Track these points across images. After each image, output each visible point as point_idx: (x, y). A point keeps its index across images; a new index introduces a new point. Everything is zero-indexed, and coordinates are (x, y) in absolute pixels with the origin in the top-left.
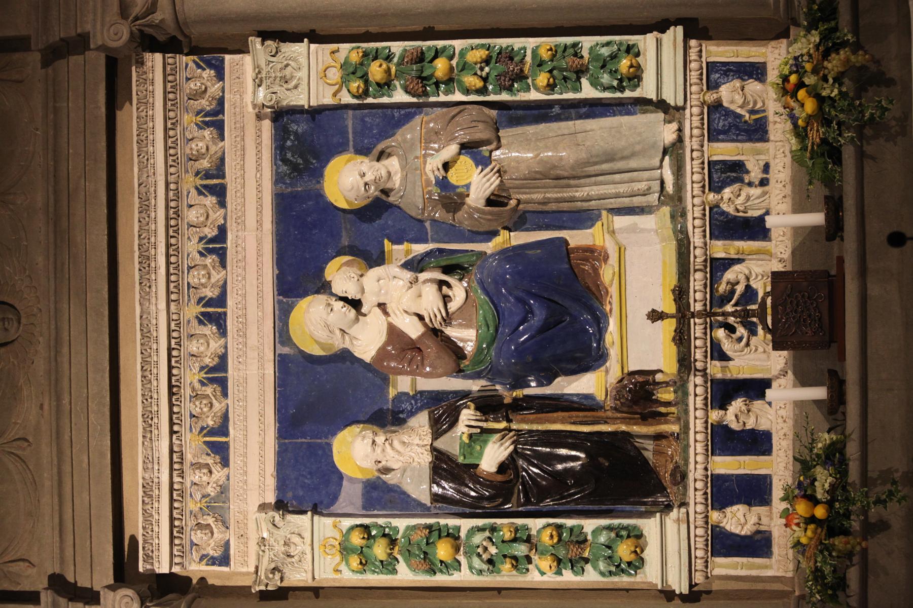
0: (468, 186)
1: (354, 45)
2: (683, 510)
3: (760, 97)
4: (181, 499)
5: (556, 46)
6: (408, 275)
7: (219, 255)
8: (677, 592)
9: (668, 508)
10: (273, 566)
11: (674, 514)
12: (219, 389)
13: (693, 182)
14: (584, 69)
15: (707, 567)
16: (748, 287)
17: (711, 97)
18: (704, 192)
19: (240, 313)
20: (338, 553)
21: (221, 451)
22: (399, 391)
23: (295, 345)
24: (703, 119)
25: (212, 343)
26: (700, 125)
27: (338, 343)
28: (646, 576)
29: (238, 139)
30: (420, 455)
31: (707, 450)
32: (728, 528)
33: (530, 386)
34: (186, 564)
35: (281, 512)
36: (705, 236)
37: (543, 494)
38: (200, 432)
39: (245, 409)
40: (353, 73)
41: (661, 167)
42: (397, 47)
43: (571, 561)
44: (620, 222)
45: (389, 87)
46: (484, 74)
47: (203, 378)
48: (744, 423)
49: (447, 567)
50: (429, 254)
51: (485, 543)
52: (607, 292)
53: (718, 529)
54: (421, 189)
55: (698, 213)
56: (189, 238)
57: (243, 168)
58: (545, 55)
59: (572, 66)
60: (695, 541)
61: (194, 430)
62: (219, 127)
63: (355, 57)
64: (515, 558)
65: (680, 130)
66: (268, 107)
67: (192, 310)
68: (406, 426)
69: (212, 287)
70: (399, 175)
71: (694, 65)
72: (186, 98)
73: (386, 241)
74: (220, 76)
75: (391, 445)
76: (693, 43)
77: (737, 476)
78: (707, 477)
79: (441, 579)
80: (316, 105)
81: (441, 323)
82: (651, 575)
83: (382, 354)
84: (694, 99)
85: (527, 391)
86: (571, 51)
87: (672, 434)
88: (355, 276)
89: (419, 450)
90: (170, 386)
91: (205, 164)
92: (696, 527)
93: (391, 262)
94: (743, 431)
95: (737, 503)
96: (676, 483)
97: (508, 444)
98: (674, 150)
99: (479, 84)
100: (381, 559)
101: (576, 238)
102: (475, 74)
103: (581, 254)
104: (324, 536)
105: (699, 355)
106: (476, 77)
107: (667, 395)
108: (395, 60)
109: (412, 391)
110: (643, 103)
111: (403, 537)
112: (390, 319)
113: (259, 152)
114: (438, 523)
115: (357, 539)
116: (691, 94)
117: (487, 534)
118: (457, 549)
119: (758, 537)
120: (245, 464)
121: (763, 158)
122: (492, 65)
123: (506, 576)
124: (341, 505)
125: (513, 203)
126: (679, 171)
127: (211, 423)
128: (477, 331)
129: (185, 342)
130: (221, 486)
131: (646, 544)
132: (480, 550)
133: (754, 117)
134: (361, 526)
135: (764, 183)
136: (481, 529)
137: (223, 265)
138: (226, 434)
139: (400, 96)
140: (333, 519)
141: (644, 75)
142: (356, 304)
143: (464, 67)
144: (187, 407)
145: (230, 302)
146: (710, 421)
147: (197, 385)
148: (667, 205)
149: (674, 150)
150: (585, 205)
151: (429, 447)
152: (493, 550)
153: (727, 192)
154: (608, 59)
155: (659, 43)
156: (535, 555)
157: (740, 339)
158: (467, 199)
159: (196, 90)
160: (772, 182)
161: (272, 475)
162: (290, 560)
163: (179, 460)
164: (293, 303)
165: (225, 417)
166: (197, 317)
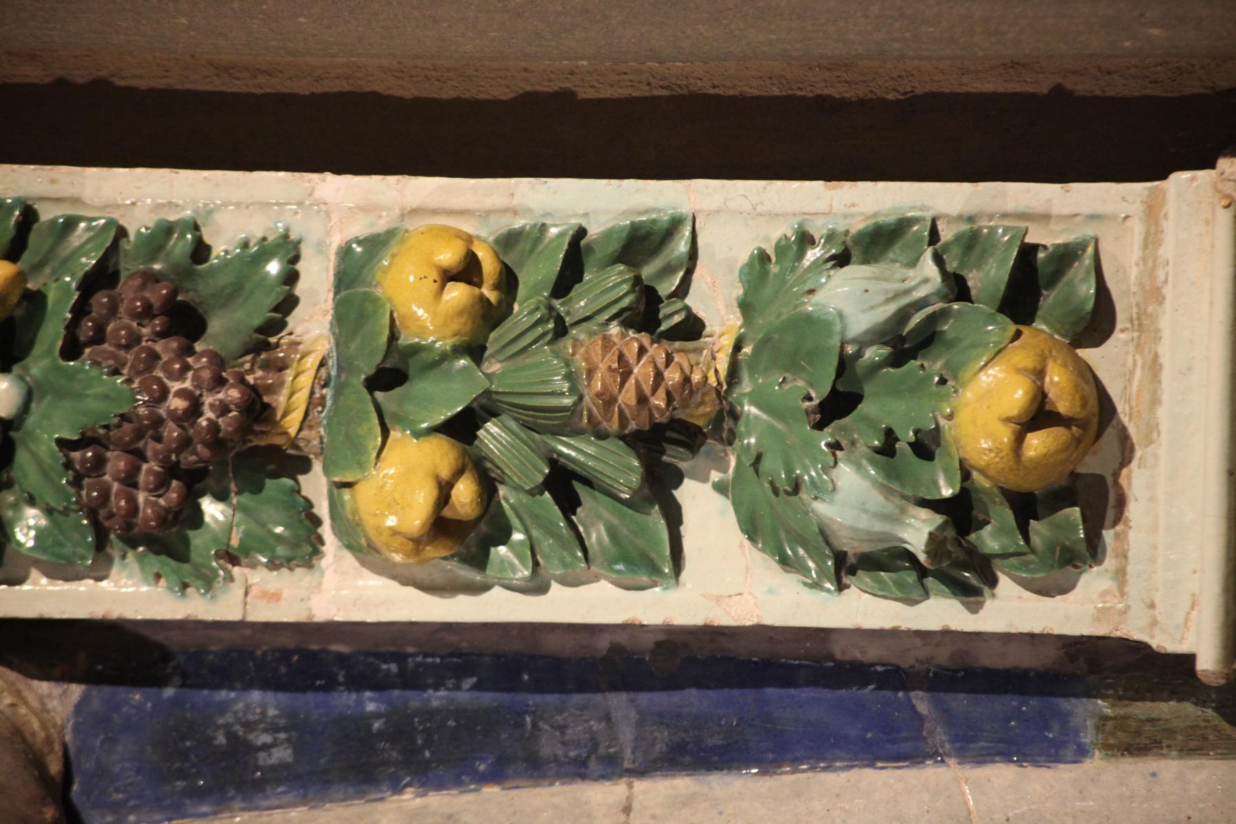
5: (508, 241)
14: (700, 414)
59: (608, 401)
154: (873, 354)
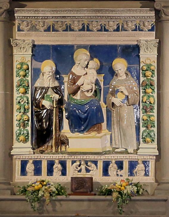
0: (117, 98)
2: (33, 153)
5: (154, 121)
6: (94, 81)
8: (11, 151)
9: (34, 149)
10: (18, 44)
12: (65, 29)
13: (118, 156)
15: (18, 159)
17: (140, 162)
18: (115, 159)
19: (85, 35)
21: (48, 30)
24: (134, 159)
27: (77, 62)
28: (16, 143)
29: (132, 35)
32: (28, 165)
34: (18, 20)
38: (54, 24)
40: (148, 67)
41: (122, 148)
42: (155, 79)
43: (20, 123)
44: (108, 137)
45: (144, 76)
46: (147, 102)
48: (55, 169)
49: (18, 91)
50: (100, 86)
51: (24, 101)
52: (89, 133)
58: (152, 118)
62: (135, 30)
63: (152, 68)
64: (20, 109)
68: (55, 80)
70: (121, 79)
71: (148, 157)
73: (104, 75)
75: (49, 76)
76: (155, 157)
77: (41, 167)
79: (15, 88)
80: (140, 56)
82: (16, 144)
83: (73, 74)
84: (139, 157)
85: (64, 112)
87: (52, 150)
89: (48, 84)
90: (65, 17)
91: (125, 26)
92: (28, 156)
94: (53, 168)
95: (35, 167)
97: (50, 107)
98: (126, 152)
99: (144, 101)
101: (104, 124)
102: (147, 100)
103: (100, 126)
105: (73, 157)
108: (152, 78)
111: (26, 79)
112: (83, 76)
115: (25, 67)
117: (27, 102)
118: (23, 93)
122: (149, 104)
123: (16, 107)
125: (113, 109)
127: (56, 27)
128: (79, 99)
129: (77, 20)
132: (22, 100)
135: (117, 175)
136: (28, 100)
139: (142, 79)
140: (30, 60)
142: (87, 67)
143: (149, 97)
147: (66, 23)
148: (112, 149)
149: (126, 152)
151: (49, 86)
152: (22, 103)
153: (115, 165)
155: (155, 148)
157: (77, 168)
160: (118, 177)
161: (42, 44)
166: (84, 23)
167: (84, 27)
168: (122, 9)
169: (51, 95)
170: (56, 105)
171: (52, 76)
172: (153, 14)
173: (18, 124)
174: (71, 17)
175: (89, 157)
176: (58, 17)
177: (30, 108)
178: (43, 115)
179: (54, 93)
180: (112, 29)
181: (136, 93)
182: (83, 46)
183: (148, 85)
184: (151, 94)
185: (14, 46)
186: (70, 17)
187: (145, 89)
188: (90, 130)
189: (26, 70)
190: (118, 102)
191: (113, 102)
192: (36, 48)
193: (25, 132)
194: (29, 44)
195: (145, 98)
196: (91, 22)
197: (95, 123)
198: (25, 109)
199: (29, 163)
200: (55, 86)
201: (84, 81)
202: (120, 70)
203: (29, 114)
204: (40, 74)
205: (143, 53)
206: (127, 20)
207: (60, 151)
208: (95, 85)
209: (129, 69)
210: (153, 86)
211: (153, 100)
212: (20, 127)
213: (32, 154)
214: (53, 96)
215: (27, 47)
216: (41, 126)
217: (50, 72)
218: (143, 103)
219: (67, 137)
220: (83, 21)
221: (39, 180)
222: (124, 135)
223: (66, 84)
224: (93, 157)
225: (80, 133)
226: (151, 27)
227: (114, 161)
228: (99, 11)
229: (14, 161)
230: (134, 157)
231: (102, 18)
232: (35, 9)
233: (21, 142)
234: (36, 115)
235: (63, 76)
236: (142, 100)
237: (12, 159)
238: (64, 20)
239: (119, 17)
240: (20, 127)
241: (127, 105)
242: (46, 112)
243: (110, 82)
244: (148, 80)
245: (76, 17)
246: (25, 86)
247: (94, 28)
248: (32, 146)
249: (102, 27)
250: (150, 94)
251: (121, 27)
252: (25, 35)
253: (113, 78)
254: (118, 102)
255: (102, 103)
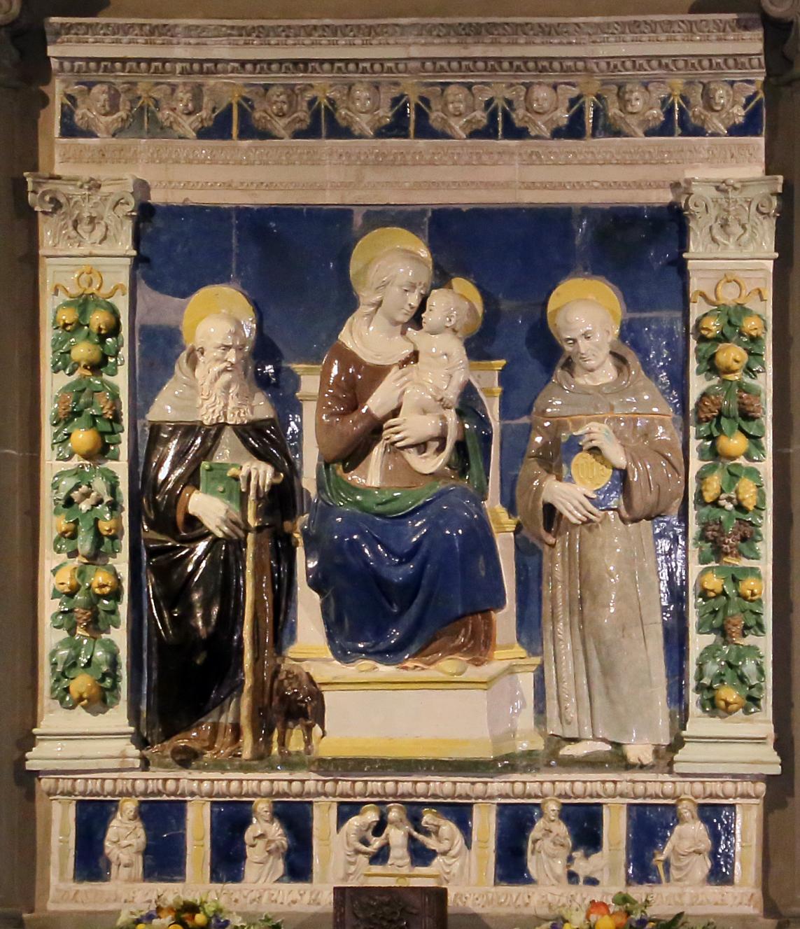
0: (570, 479)
1: (770, 322)
2: (138, 763)
3: (686, 875)
4: (152, 71)
5: (760, 600)
6: (452, 395)
7: (487, 127)
8: (28, 755)
9: (142, 742)
10: (62, 200)
11: (133, 751)
12: (304, 126)
13: (573, 782)
14: (728, 638)
15: (62, 794)
16: (433, 854)
17: (686, 809)
18: (560, 796)
19: (409, 157)
20: (81, 291)
21: (218, 129)
22: (302, 377)
23: (365, 234)
24: (657, 797)
25: (367, 117)
26: (648, 793)
27: (366, 297)
28: (51, 711)
29: (647, 156)
30: (211, 410)
31: (218, 795)
33: (307, 555)
34: (63, 76)
35: (134, 214)
36: (500, 796)
37: (162, 573)
38: (246, 100)
39: (278, 163)
40: (729, 322)
41: (596, 739)
42: (765, 382)
43: (71, 611)
44: (526, 681)
45: (709, 371)
46: (722, 502)
47: (320, 104)
48: (253, 846)
49: (63, 441)
50: (484, 423)
51: (93, 494)
52: (430, 664)
53: (113, 809)
54: (569, 413)
55: (532, 788)
56: (512, 85)
57: (606, 163)
58: (748, 585)
59: (729, 622)
60: (97, 779)
61: (247, 90)
62: (664, 129)
63: (750, 325)
64: (74, 536)
65: (642, 767)
66: (687, 201)
67: (412, 90)
68: (255, 387)
69: (442, 118)
70: (590, 383)
71: (729, 787)
72: (705, 81)
73: (503, 362)
74: (735, 131)
75: (225, 370)
76: (761, 787)
77: (184, 836)
78: (182, 795)
79: (48, 432)
80: (689, 267)
81: (388, 439)
82: (52, 718)
83: (348, 358)
84: (684, 787)
85: (300, 552)
86: (752, 622)
88: (453, 323)
89: (219, 407)
90: (306, 62)
91: (614, 110)
92: (115, 780)
93: (471, 368)
94: (244, 844)
95: (146, 835)
96: (176, 751)
97: (226, 529)
98: (617, 759)
99: (709, 497)
100: (72, 353)
101: (505, 620)
102: (722, 491)
103: (483, 627)
104: (105, 272)
105: (344, 786)
106: (718, 491)
107: (296, 741)
108: (747, 380)
109: (300, 396)
110: (681, 716)
111: (103, 382)
112: (395, 369)
113: (628, 185)
114: (122, 431)
115: (98, 319)
116: (691, 782)
117: (107, 499)
118: (87, 456)
119: (102, 864)
120: (202, 162)
121: (604, 878)
122: (735, 512)
123: (52, 524)
124: (147, 296)
125: (551, 540)
126: (591, 763)
127: (257, 115)
128: (378, 489)
129: (367, 78)
130: (171, 127)
131: (95, 713)
132: (84, 488)
133: (660, 867)
134: (118, 325)
135: (572, 877)
136: (113, 490)
137: (474, 134)
138: (243, 135)
139: (697, 385)
140: (127, 284)
141: (717, 719)
142: (416, 321)
143: (734, 476)
144: (277, 77)
145: (422, 143)
146: (256, 800)
147: (309, 95)
148: (546, 746)
149: (617, 759)
150: (547, 636)
151: (222, 421)
152: (84, 506)
153: (561, 829)
154: (739, 672)
155: (760, 741)
156: (79, 561)
157: (365, 842)
158: (554, 478)
159: (714, 98)
160: (573, 890)
161: (187, 199)
162: (70, 223)
163: (205, 70)
164: (423, 231)
165: (265, 135)
166: (402, 96)
167: (401, 115)
168: (597, 19)
169: (234, 465)
170: (257, 516)
171: (240, 368)
172: (752, 43)
173: (64, 612)
174: (337, 65)
175: (428, 782)
176: (270, 62)
177: (122, 533)
178: (190, 568)
179: (247, 454)
180: (545, 124)
181: (667, 458)
182: (401, 212)
183: (728, 417)
184: (742, 461)
185: (45, 213)
186: (332, 62)
187: (716, 434)
188: (433, 646)
189: (102, 338)
190: (576, 503)
191: (549, 500)
192: (158, 222)
193: (99, 653)
194: (117, 203)
195: (714, 484)
196: (438, 89)
197: (460, 612)
198: (98, 537)
199: (119, 814)
200: (252, 417)
201: (403, 393)
202: (586, 336)
203: (121, 563)
204: (177, 356)
205: (701, 249)
206: (620, 79)
207: (280, 753)
208: (460, 413)
209: (630, 334)
210: (753, 419)
211: (754, 490)
212: (72, 631)
213: (133, 769)
214: (244, 473)
215: (109, 216)
216: (183, 623)
217: (227, 348)
218: (705, 510)
219: (317, 679)
220: (396, 84)
221: (170, 899)
222: (608, 671)
223: (309, 410)
224: (448, 787)
225: (381, 662)
226: (743, 113)
227: (552, 807)
228: (476, 32)
229: (40, 806)
230: (656, 786)
231: (494, 70)
232: (155, 22)
233: (79, 708)
234: (156, 570)
235: (298, 367)
236: (700, 494)
237: (31, 795)
238: (299, 79)
239: (580, 64)
240: (72, 631)
241: (623, 520)
242: (205, 553)
243: (538, 401)
244: (729, 390)
245: (361, 65)
246: (100, 417)
247: (452, 122)
248: (132, 729)
249: (493, 116)
250: (737, 461)
251: (590, 114)
252: (102, 156)
253: (549, 380)
254: (576, 503)
255: (493, 505)
